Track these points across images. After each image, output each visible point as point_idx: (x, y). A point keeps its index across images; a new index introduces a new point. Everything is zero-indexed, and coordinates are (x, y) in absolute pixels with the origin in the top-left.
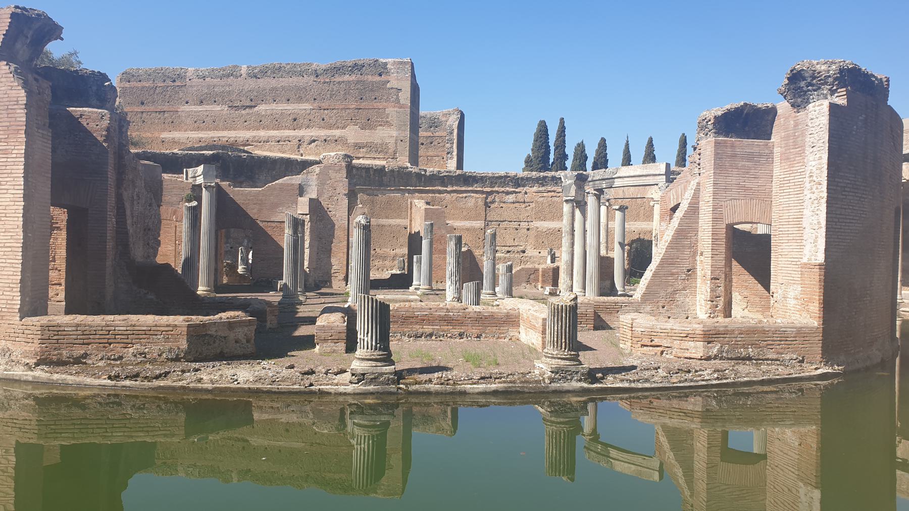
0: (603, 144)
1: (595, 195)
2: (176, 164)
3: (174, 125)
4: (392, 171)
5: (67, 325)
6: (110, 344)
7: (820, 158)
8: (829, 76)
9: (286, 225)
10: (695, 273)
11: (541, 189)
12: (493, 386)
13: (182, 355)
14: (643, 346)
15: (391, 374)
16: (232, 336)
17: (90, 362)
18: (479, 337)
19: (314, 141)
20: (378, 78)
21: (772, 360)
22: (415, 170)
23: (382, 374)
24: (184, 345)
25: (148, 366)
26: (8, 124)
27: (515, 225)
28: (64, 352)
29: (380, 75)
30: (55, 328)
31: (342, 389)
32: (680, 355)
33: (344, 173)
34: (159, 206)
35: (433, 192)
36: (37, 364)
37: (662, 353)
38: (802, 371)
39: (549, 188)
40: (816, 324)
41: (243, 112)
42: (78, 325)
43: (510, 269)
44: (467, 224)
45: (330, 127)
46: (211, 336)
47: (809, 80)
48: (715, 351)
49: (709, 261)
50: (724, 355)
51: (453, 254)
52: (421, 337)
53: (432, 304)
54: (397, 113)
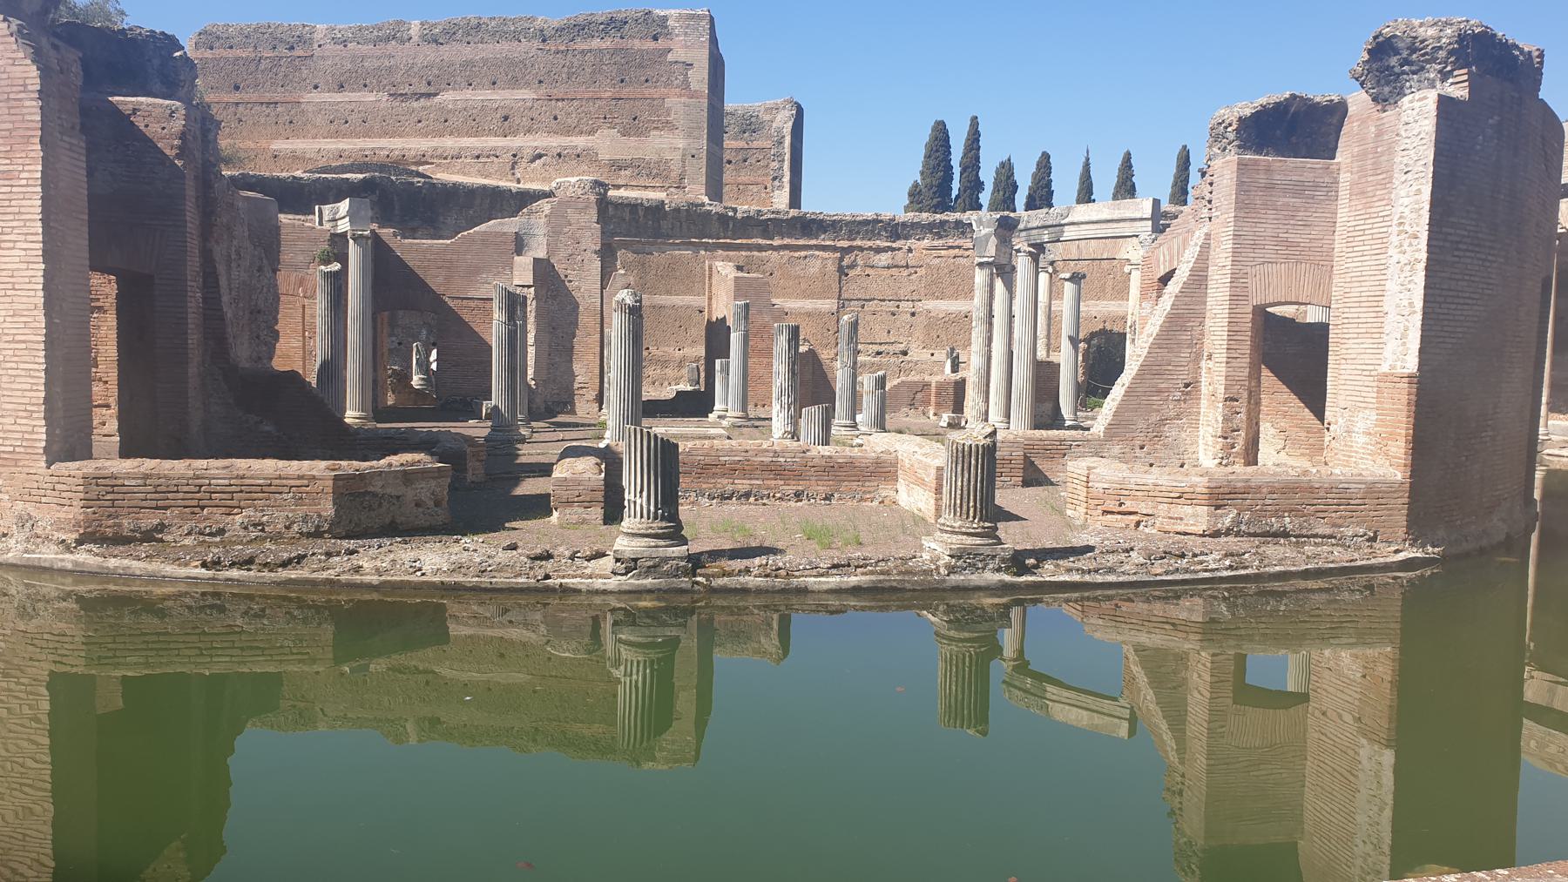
0: (1045, 164)
1: (1030, 253)
2: (301, 196)
3: (294, 127)
4: (677, 210)
5: (129, 476)
6: (203, 508)
7: (1418, 192)
8: (1440, 48)
9: (495, 305)
10: (1197, 389)
11: (936, 243)
12: (853, 578)
13: (326, 527)
14: (1105, 512)
15: (681, 558)
16: (409, 494)
17: (169, 538)
18: (828, 498)
19: (540, 156)
20: (650, 45)
21: (1323, 537)
22: (716, 208)
23: (666, 560)
24: (328, 509)
25: (268, 545)
26: (10, 126)
27: (891, 306)
28: (125, 522)
29: (655, 38)
31: (598, 584)
32: (1168, 528)
33: (593, 213)
34: (275, 271)
35: (749, 248)
36: (80, 542)
37: (1138, 524)
38: (1373, 554)
39: (951, 242)
40: (1399, 477)
41: (415, 104)
42: (146, 477)
43: (881, 383)
44: (808, 304)
45: (569, 131)
46: (375, 495)
47: (1405, 54)
48: (1228, 521)
49: (1223, 368)
50: (1243, 528)
51: (785, 357)
52: (730, 498)
53: (750, 444)
54: (684, 107)
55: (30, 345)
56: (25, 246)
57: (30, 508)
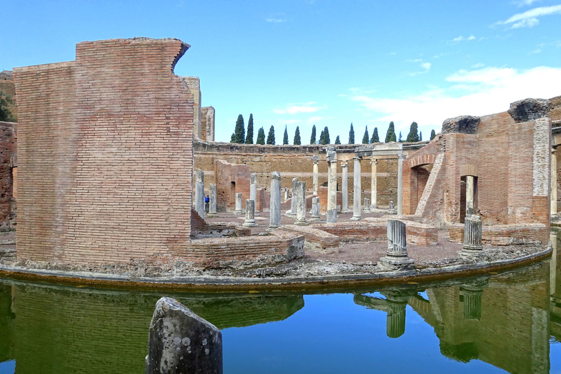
5: (222, 245)
6: (246, 255)
10: (443, 201)
23: (409, 264)
26: (179, 115)
30: (216, 247)
35: (212, 154)
36: (204, 270)
42: (228, 245)
47: (532, 107)
48: (511, 241)
55: (184, 197)
57: (182, 259)
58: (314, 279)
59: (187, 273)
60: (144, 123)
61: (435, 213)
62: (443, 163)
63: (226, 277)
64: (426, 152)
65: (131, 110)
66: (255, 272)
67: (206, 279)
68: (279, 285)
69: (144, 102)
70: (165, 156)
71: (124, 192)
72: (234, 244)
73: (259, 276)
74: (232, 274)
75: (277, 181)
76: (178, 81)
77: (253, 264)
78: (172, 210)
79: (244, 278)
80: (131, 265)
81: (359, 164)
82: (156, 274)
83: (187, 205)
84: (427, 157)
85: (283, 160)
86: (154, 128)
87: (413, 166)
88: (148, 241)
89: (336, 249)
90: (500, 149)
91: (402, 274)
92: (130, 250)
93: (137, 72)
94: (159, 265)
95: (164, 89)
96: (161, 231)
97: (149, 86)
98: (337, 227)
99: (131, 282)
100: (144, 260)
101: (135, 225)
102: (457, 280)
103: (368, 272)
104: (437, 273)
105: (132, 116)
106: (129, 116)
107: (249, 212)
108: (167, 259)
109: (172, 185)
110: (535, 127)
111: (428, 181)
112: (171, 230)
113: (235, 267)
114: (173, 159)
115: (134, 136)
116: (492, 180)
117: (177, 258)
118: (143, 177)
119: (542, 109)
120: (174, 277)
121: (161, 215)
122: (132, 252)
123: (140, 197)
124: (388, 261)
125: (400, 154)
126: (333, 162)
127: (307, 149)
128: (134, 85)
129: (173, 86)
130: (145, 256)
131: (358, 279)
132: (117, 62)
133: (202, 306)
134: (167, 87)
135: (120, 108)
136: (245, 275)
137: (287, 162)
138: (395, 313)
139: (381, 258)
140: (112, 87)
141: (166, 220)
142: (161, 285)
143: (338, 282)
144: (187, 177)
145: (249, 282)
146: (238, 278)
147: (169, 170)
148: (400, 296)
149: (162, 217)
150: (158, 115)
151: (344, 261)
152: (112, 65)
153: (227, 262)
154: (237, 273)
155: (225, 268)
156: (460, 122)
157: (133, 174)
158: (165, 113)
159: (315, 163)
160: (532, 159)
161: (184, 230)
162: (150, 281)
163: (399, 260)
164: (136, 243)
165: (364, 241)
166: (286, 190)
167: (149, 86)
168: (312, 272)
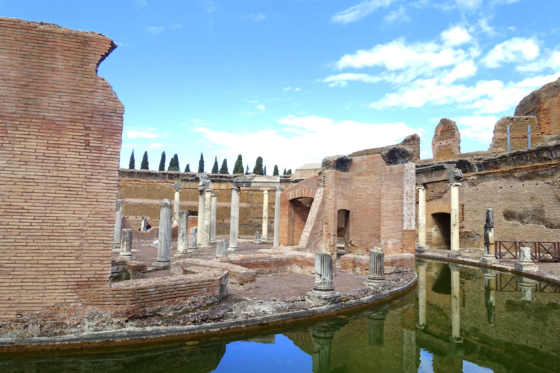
0: (225, 162)
5: (150, 287)
6: (175, 298)
11: (130, 179)
14: (366, 270)
26: (104, 127)
28: (147, 309)
30: (142, 291)
36: (126, 321)
39: (135, 179)
42: (157, 287)
55: (104, 228)
56: (107, 182)
58: (253, 321)
59: (104, 327)
60: (51, 132)
61: (316, 244)
62: (323, 197)
63: (155, 327)
64: (304, 186)
65: (33, 113)
66: (188, 318)
67: (129, 332)
68: (218, 331)
69: (54, 104)
70: (81, 176)
71: (14, 221)
72: (164, 286)
73: (194, 322)
74: (162, 323)
75: (168, 209)
76: (105, 85)
77: (184, 309)
78: (86, 245)
79: (178, 327)
80: (17, 321)
81: (237, 194)
82: (58, 331)
83: (108, 238)
84: (305, 190)
85: (140, 186)
86: (66, 140)
87: (291, 198)
88: (47, 288)
89: (253, 285)
90: (369, 187)
91: (332, 308)
92: (16, 301)
93: (45, 65)
94: (62, 319)
95: (85, 93)
96: (68, 273)
97: (63, 85)
98: (243, 260)
99: (17, 346)
100: (38, 315)
101: (27, 265)
102: (370, 310)
103: (303, 309)
104: (357, 304)
105: (33, 120)
106: (29, 120)
107: (125, 243)
108: (75, 310)
109: (89, 213)
110: (404, 170)
111: (310, 214)
112: (83, 271)
113: (163, 314)
114: (92, 180)
115: (34, 147)
116: (363, 214)
117: (90, 308)
118: (46, 202)
119: (409, 156)
120: (84, 334)
121: (70, 251)
122: (20, 303)
123: (39, 227)
124: (317, 295)
125: (278, 186)
126: (208, 191)
127: (167, 176)
128: (40, 81)
129: (98, 91)
130: (41, 308)
131: (295, 316)
132: (14, 48)
133: (122, 368)
134: (89, 90)
135: (15, 108)
136: (178, 323)
137: (144, 188)
138: (323, 349)
139: (309, 293)
140: (5, 80)
141: (77, 258)
142: (65, 345)
143: (277, 322)
144: (110, 204)
145: (183, 331)
146: (170, 327)
147: (86, 193)
148: (329, 331)
149: (71, 255)
150: (73, 124)
151: (275, 298)
152: (7, 51)
153: (154, 308)
154: (168, 321)
155: (152, 317)
156: (337, 160)
157: (29, 197)
158: (85, 122)
159: (177, 191)
160: (402, 198)
161: (103, 270)
162: (48, 341)
163: (328, 295)
164: (28, 290)
165: (267, 274)
166: (143, 218)
167: (63, 85)
168: (249, 313)
